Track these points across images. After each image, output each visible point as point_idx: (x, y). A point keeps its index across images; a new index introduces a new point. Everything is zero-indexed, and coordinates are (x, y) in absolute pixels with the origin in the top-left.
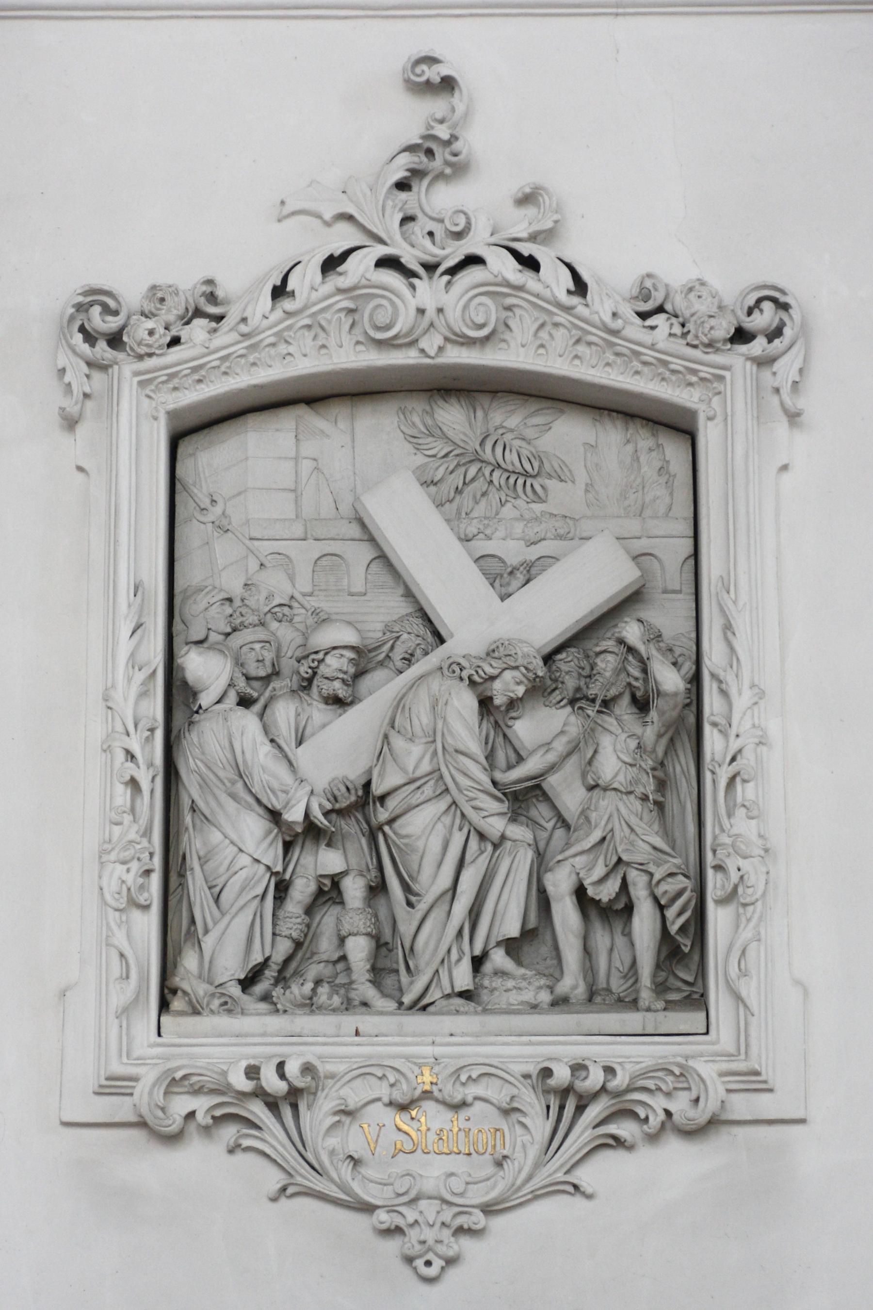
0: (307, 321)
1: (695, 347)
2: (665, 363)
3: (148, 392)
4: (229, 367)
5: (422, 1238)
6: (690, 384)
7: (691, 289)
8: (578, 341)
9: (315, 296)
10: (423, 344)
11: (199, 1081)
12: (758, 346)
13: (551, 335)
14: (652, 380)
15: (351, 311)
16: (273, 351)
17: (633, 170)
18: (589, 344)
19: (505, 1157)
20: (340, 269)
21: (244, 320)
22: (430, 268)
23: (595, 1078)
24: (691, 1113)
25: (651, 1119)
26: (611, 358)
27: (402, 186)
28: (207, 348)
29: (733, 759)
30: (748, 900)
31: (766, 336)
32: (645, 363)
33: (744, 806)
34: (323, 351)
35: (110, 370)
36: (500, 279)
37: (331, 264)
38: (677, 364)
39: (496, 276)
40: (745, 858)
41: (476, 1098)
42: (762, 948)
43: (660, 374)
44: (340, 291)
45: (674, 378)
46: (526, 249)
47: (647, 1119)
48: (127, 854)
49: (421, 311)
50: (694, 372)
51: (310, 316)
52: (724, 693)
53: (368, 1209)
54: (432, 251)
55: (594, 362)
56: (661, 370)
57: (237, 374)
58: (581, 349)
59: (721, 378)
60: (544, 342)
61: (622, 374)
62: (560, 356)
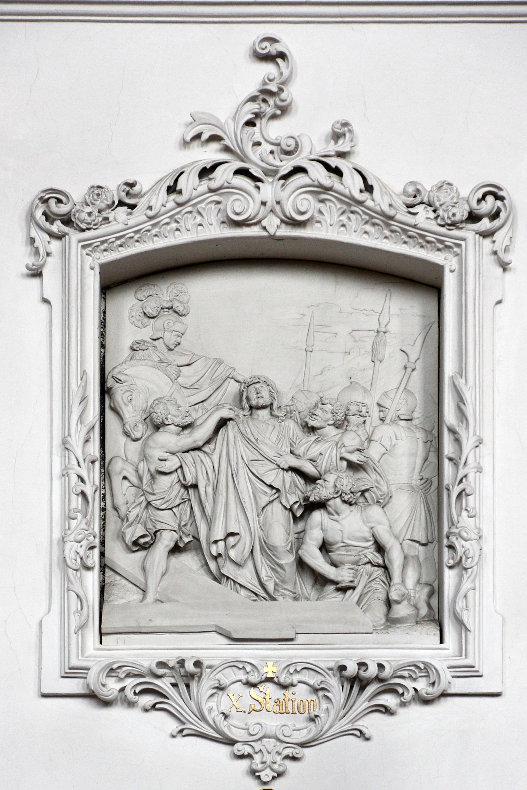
1: (443, 226)
2: (423, 237)
4: (140, 237)
5: (264, 760)
6: (439, 250)
8: (366, 223)
9: (195, 193)
11: (127, 670)
13: (349, 218)
14: (414, 247)
15: (218, 203)
16: (168, 227)
17: (408, 111)
18: (374, 224)
19: (316, 716)
20: (211, 176)
21: (150, 208)
23: (372, 671)
24: (430, 690)
25: (406, 693)
26: (387, 233)
28: (126, 225)
29: (461, 481)
30: (467, 566)
32: (410, 237)
33: (466, 510)
34: (200, 228)
35: (63, 239)
36: (316, 183)
37: (205, 173)
38: (430, 237)
39: (314, 181)
41: (300, 682)
43: (420, 243)
44: (211, 191)
45: (428, 245)
46: (334, 162)
47: (403, 694)
48: (80, 537)
49: (264, 203)
50: (442, 242)
51: (190, 206)
52: (458, 441)
53: (231, 742)
55: (376, 236)
56: (420, 241)
57: (145, 242)
58: (368, 228)
59: (459, 246)
60: (345, 223)
61: (395, 243)
62: (355, 232)
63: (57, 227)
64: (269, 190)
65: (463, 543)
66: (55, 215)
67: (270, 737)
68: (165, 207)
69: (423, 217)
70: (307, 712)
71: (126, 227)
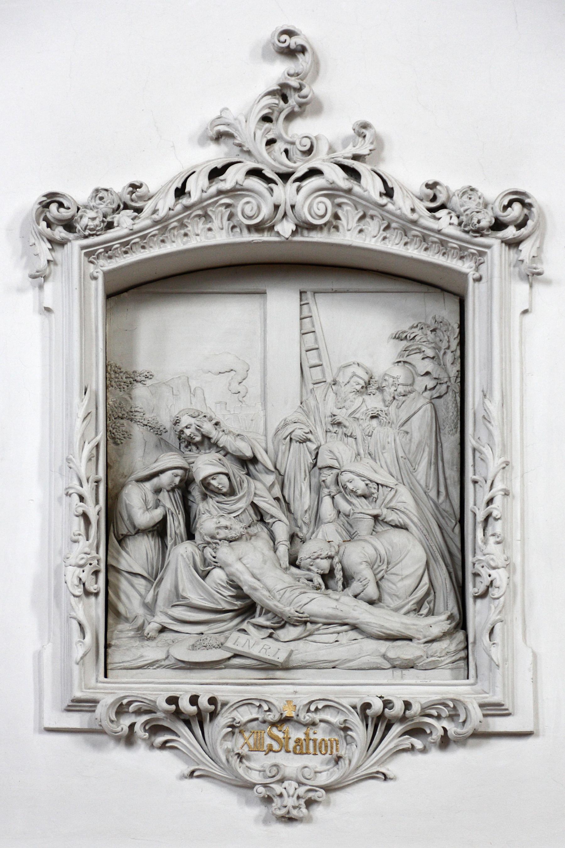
0: (199, 212)
3: (91, 259)
7: (464, 193)
9: (204, 195)
10: (277, 228)
12: (510, 232)
20: (221, 177)
22: (285, 177)
27: (266, 119)
31: (516, 226)
35: (66, 246)
37: (216, 173)
40: (494, 568)
42: (506, 626)
54: (285, 165)
63: (60, 233)
64: (285, 193)
65: (492, 572)
66: (56, 217)
67: (290, 779)
68: (173, 210)
69: (445, 222)
70: (329, 752)
71: (131, 231)
